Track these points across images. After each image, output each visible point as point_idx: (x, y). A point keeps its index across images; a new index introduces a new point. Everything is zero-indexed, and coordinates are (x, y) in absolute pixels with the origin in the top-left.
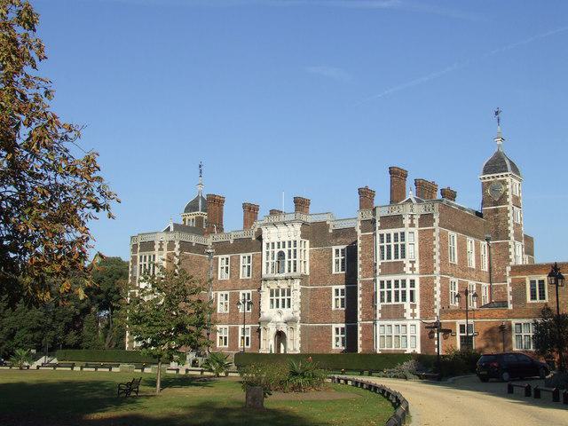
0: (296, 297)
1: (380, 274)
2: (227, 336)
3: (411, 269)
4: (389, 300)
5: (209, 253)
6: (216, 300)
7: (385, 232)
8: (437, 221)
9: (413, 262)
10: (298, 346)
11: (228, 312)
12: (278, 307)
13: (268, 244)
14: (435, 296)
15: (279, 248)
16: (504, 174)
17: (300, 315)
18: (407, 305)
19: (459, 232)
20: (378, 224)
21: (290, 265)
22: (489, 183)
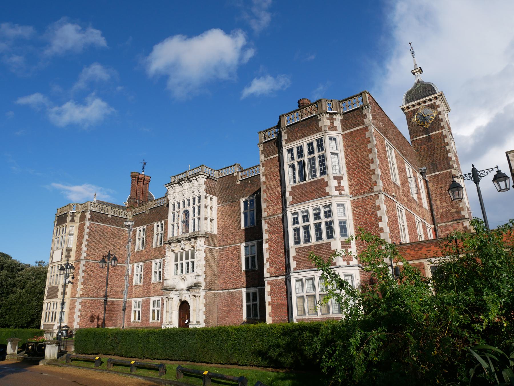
0: (200, 258)
1: (291, 204)
2: (140, 309)
3: (337, 188)
4: (308, 239)
5: (128, 226)
6: (133, 272)
7: (294, 145)
8: (370, 116)
9: (339, 179)
10: (202, 318)
11: (142, 284)
12: (182, 272)
13: (174, 205)
14: (381, 225)
15: (184, 207)
16: (432, 97)
17: (205, 280)
18: (336, 245)
19: (396, 147)
20: (285, 137)
21: (194, 224)
22: (415, 112)
